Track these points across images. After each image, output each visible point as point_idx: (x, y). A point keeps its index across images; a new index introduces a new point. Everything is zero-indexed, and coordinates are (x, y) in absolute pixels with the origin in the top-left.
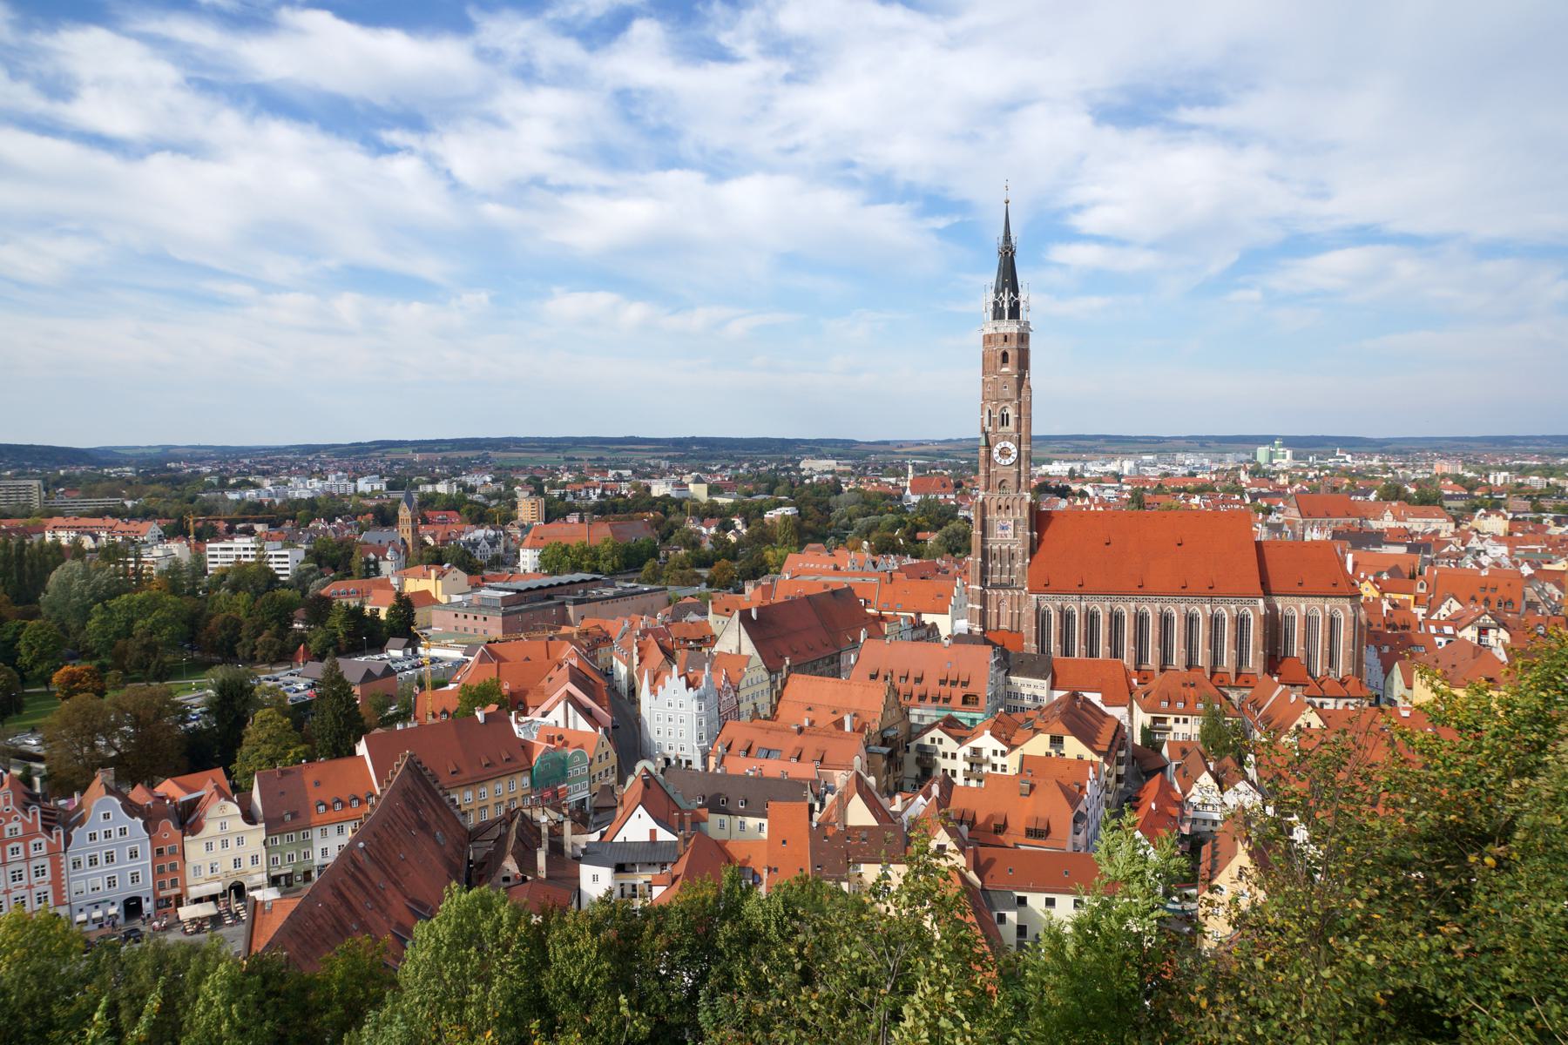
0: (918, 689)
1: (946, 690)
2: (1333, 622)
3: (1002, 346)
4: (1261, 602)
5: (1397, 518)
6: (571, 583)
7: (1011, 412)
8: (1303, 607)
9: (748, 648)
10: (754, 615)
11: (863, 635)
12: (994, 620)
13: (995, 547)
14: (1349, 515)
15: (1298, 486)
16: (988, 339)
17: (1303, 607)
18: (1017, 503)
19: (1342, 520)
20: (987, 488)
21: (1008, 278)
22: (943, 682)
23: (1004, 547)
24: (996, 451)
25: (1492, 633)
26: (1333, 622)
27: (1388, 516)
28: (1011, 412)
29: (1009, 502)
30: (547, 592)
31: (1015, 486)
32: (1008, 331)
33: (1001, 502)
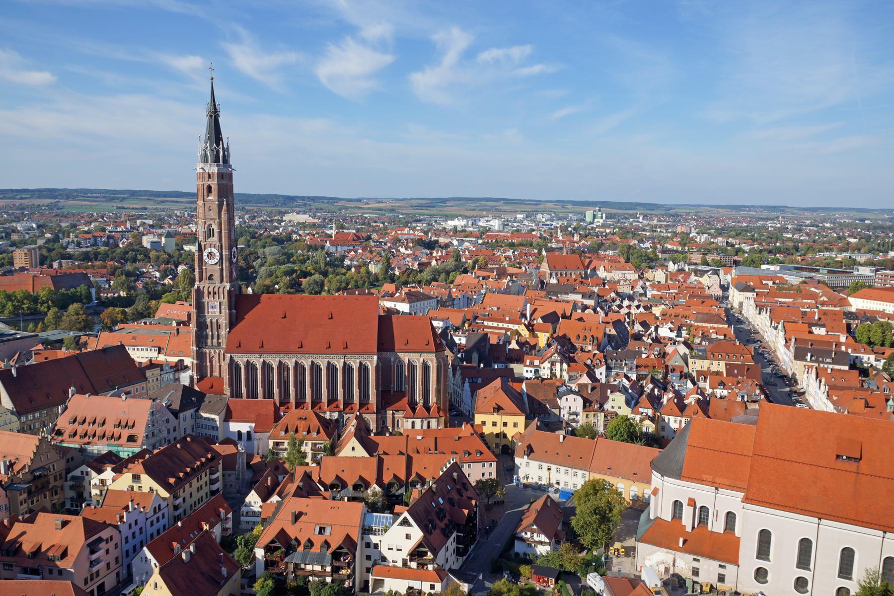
0: (99, 431)
1: (117, 431)
2: (426, 368)
4: (375, 357)
7: (215, 227)
11: (71, 390)
15: (583, 242)
18: (221, 290)
20: (201, 280)
21: (216, 134)
24: (205, 254)
25: (558, 365)
26: (426, 368)
28: (215, 227)
31: (219, 279)
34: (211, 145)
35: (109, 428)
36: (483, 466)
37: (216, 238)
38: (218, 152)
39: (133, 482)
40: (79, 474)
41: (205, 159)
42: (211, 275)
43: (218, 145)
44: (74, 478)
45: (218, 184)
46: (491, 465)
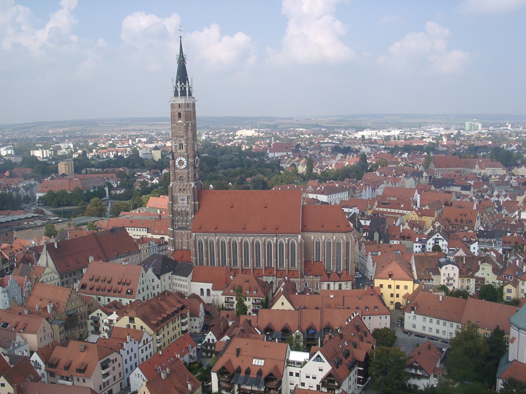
0: (108, 286)
3: (177, 110)
5: (481, 168)
6: (20, 219)
8: (323, 237)
9: (51, 263)
10: (56, 246)
11: (91, 259)
12: (180, 245)
13: (179, 209)
14: (458, 167)
16: (172, 106)
17: (323, 237)
18: (188, 188)
19: (455, 169)
21: (182, 75)
22: (119, 283)
23: (183, 209)
27: (477, 166)
29: (184, 187)
30: (5, 225)
32: (180, 102)
33: (181, 187)
34: (181, 84)
35: (114, 285)
36: (380, 318)
37: (184, 150)
38: (185, 88)
39: (130, 322)
40: (96, 316)
41: (176, 95)
43: (185, 84)
44: (93, 318)
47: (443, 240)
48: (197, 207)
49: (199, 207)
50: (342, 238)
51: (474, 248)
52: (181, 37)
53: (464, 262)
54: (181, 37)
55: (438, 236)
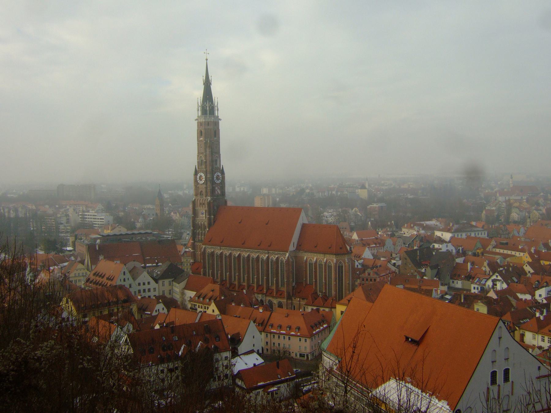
23: (202, 223)
33: (201, 201)
36: (300, 340)
42: (201, 191)
45: (205, 129)
46: (306, 341)
47: (503, 283)
48: (212, 221)
49: (214, 222)
50: (333, 261)
51: (540, 295)
52: (207, 60)
53: (462, 301)
54: (207, 60)
55: (497, 276)
